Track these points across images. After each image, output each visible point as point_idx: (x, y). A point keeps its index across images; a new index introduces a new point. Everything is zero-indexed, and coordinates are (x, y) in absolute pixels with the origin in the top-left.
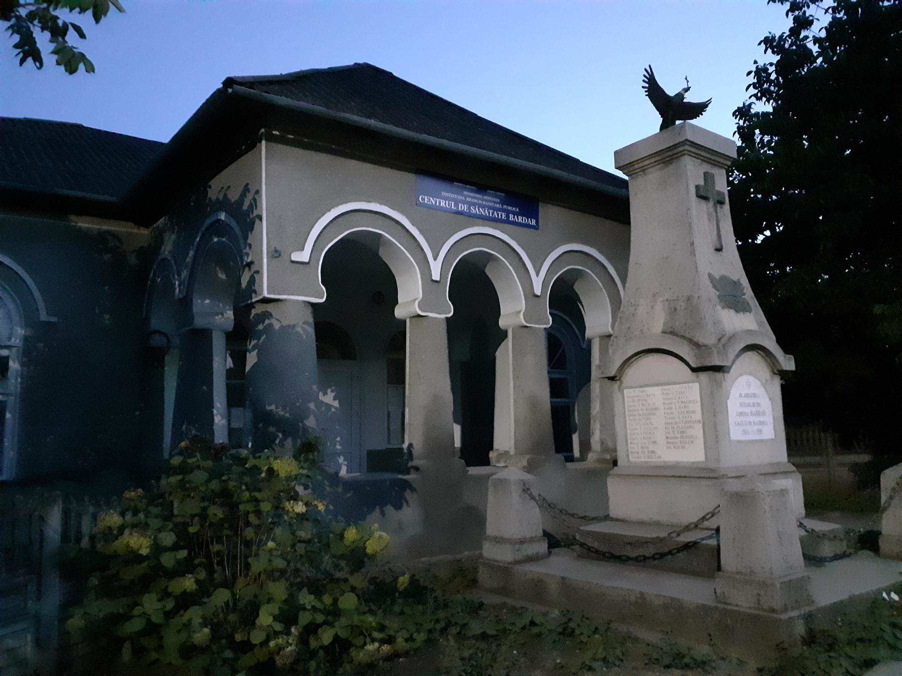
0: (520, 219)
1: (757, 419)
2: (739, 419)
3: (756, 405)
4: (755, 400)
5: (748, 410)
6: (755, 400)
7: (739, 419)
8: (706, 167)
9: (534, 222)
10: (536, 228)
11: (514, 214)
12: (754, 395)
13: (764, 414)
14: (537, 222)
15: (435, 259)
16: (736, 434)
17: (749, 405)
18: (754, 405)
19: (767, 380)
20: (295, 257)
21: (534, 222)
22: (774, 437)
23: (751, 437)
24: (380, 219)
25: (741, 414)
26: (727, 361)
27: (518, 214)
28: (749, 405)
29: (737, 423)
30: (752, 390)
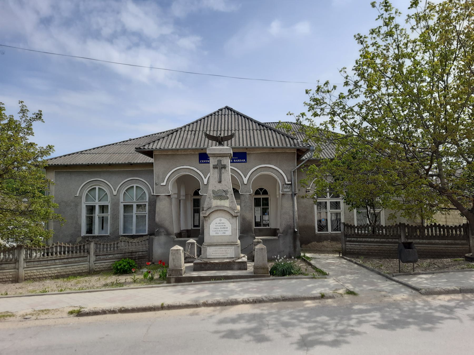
0: (238, 161)
1: (224, 229)
2: (215, 230)
4: (223, 224)
5: (220, 227)
6: (223, 224)
7: (215, 230)
8: (219, 158)
9: (244, 160)
10: (246, 162)
11: (236, 159)
12: (223, 223)
13: (227, 228)
14: (246, 160)
15: (205, 178)
16: (212, 233)
17: (220, 226)
18: (222, 226)
19: (230, 219)
20: (162, 184)
21: (244, 160)
22: (231, 234)
23: (220, 234)
24: (187, 170)
25: (216, 228)
27: (237, 159)
28: (220, 226)
30: (222, 222)
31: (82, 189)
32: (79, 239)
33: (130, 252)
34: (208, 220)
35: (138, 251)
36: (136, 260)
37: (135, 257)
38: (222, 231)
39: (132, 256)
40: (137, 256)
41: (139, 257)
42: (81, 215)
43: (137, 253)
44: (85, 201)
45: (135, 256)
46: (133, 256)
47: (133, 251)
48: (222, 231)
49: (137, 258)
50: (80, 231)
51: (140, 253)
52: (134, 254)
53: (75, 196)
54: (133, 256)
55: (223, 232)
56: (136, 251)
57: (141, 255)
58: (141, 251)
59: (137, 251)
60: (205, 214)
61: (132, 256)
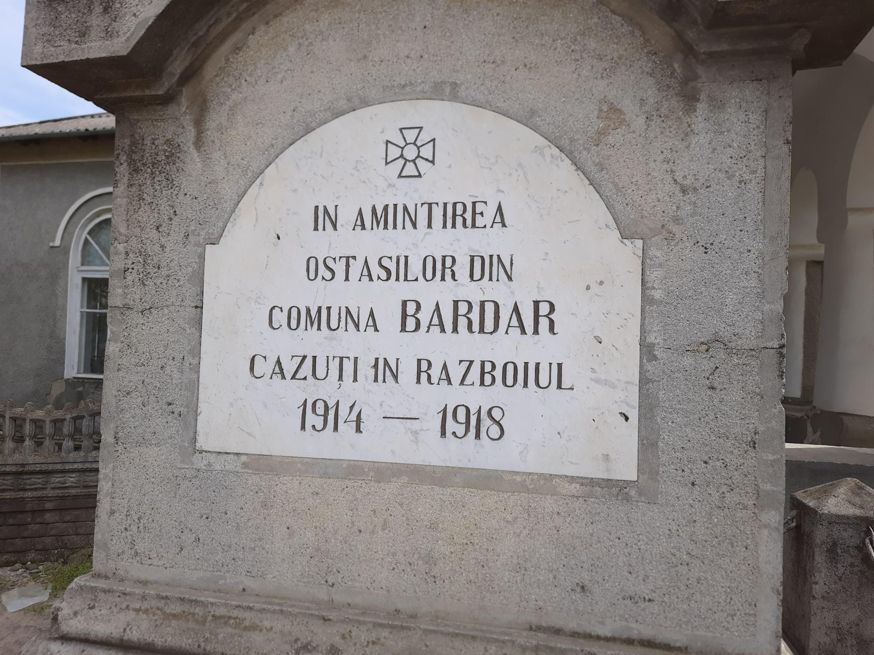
3: (462, 270)
26: (108, 34)
29: (263, 368)
31: (71, 223)
32: (57, 389)
33: (8, 469)
34: (173, 153)
35: (59, 467)
36: (48, 517)
37: (40, 498)
38: (422, 369)
39: (21, 494)
40: (51, 493)
41: (63, 498)
42: (64, 308)
43: (56, 480)
44: (79, 264)
45: (39, 494)
46: (29, 494)
47: (27, 468)
48: (422, 369)
49: (48, 505)
50: (60, 362)
51: (72, 479)
52: (38, 480)
53: (51, 244)
54: (29, 494)
55: (454, 395)
56: (44, 467)
57: (73, 492)
58: (76, 466)
59: (50, 467)
60: (96, 20)
61: (21, 494)
